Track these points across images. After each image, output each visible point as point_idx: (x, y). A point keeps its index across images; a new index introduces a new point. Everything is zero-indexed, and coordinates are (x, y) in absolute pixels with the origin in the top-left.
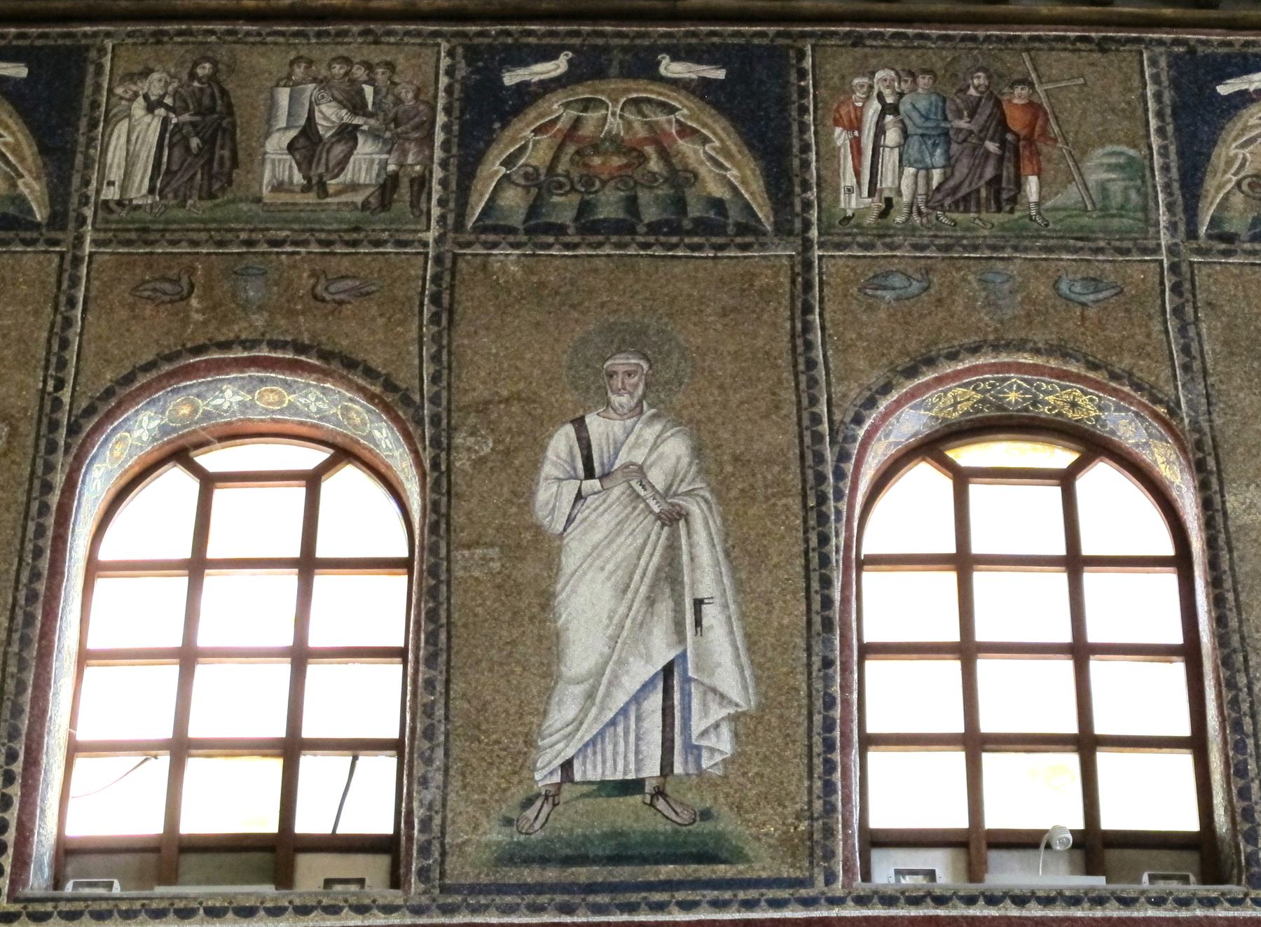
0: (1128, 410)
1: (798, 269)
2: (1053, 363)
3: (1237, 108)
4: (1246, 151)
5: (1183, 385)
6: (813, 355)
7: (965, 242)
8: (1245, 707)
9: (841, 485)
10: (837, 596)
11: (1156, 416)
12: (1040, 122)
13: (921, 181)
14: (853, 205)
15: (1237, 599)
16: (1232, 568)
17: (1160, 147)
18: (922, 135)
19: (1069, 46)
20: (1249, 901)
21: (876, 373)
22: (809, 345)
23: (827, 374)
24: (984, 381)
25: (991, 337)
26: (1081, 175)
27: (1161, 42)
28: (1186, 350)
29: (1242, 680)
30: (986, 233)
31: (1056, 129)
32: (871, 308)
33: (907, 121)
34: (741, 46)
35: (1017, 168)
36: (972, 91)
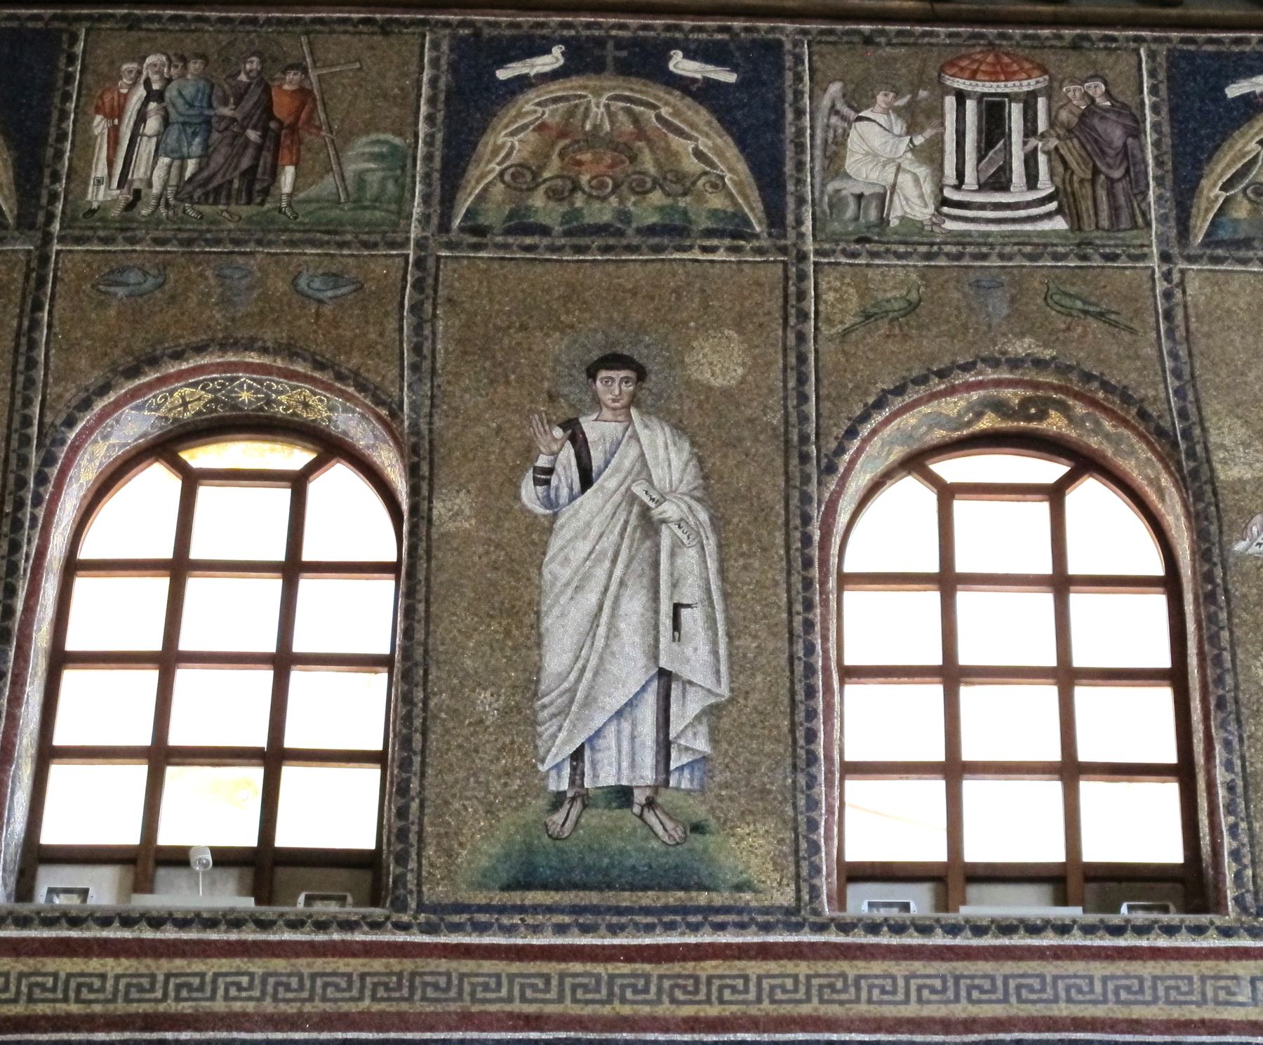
0: (354, 412)
1: (34, 264)
2: (279, 363)
3: (513, 93)
4: (515, 139)
5: (410, 386)
6: (34, 354)
7: (209, 236)
8: (417, 723)
9: (41, 490)
10: (20, 606)
11: (379, 418)
12: (307, 109)
13: (174, 171)
14: (101, 197)
15: (427, 611)
16: (427, 579)
17: (426, 135)
18: (184, 124)
19: (351, 29)
20: (389, 925)
21: (96, 373)
22: (32, 344)
23: (46, 375)
24: (213, 380)
25: (220, 335)
26: (339, 164)
27: (447, 24)
28: (417, 349)
29: (419, 694)
30: (232, 226)
31: (322, 116)
32: (102, 305)
33: (170, 109)
34: (13, 29)
35: (276, 158)
36: (243, 77)
